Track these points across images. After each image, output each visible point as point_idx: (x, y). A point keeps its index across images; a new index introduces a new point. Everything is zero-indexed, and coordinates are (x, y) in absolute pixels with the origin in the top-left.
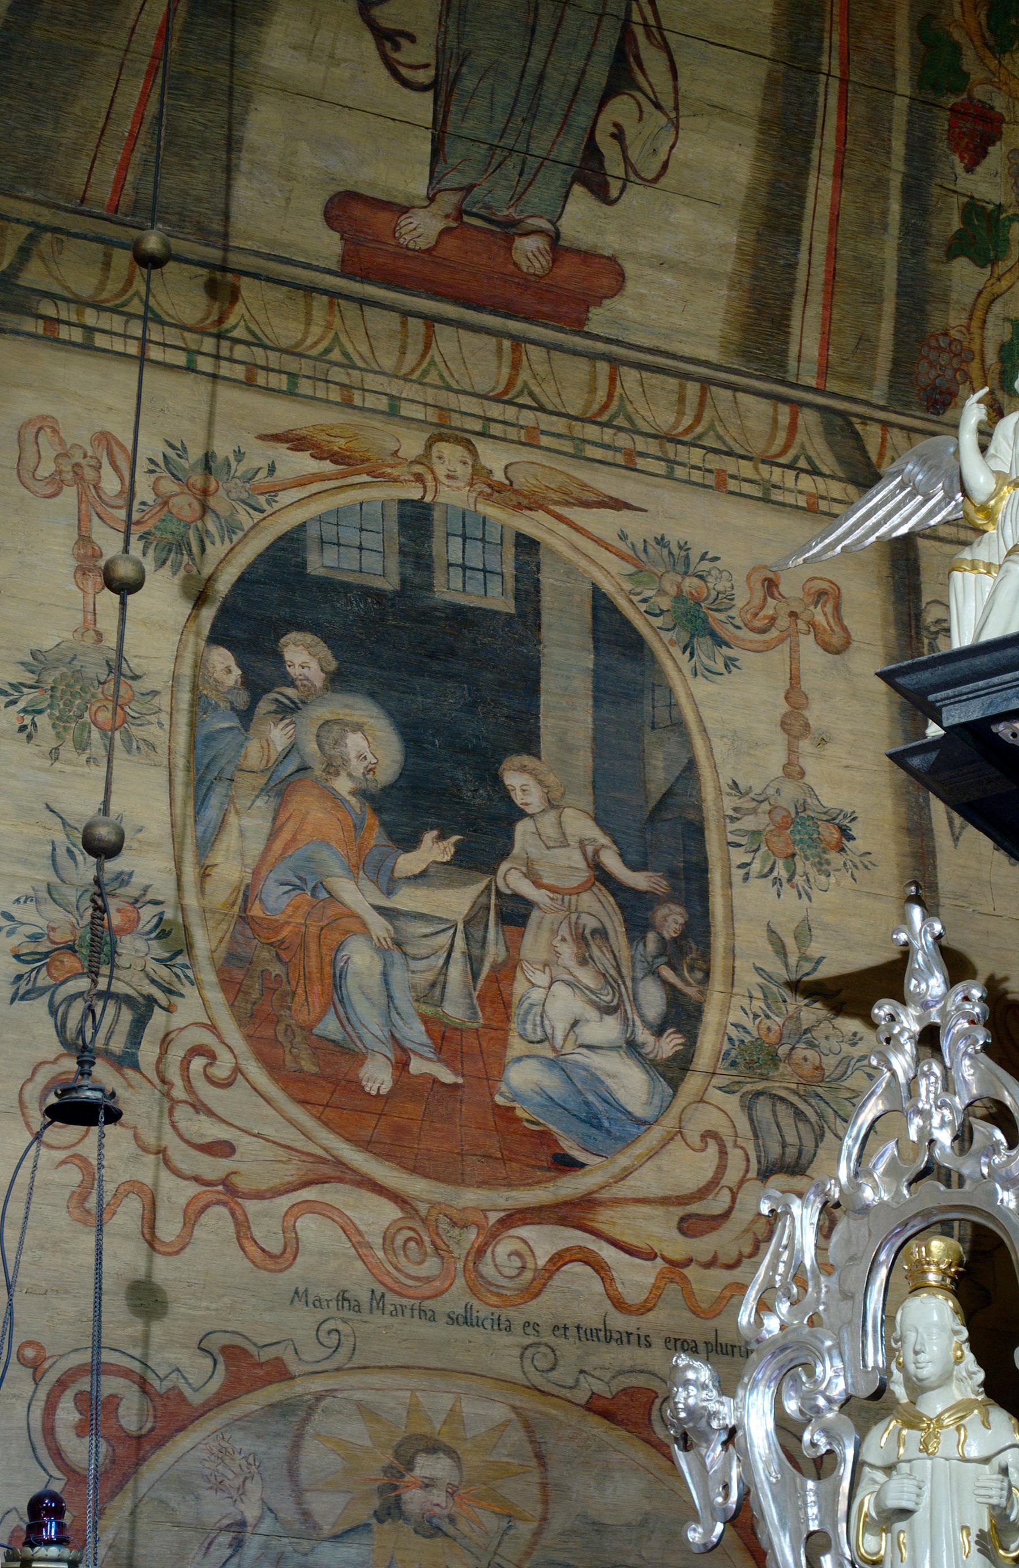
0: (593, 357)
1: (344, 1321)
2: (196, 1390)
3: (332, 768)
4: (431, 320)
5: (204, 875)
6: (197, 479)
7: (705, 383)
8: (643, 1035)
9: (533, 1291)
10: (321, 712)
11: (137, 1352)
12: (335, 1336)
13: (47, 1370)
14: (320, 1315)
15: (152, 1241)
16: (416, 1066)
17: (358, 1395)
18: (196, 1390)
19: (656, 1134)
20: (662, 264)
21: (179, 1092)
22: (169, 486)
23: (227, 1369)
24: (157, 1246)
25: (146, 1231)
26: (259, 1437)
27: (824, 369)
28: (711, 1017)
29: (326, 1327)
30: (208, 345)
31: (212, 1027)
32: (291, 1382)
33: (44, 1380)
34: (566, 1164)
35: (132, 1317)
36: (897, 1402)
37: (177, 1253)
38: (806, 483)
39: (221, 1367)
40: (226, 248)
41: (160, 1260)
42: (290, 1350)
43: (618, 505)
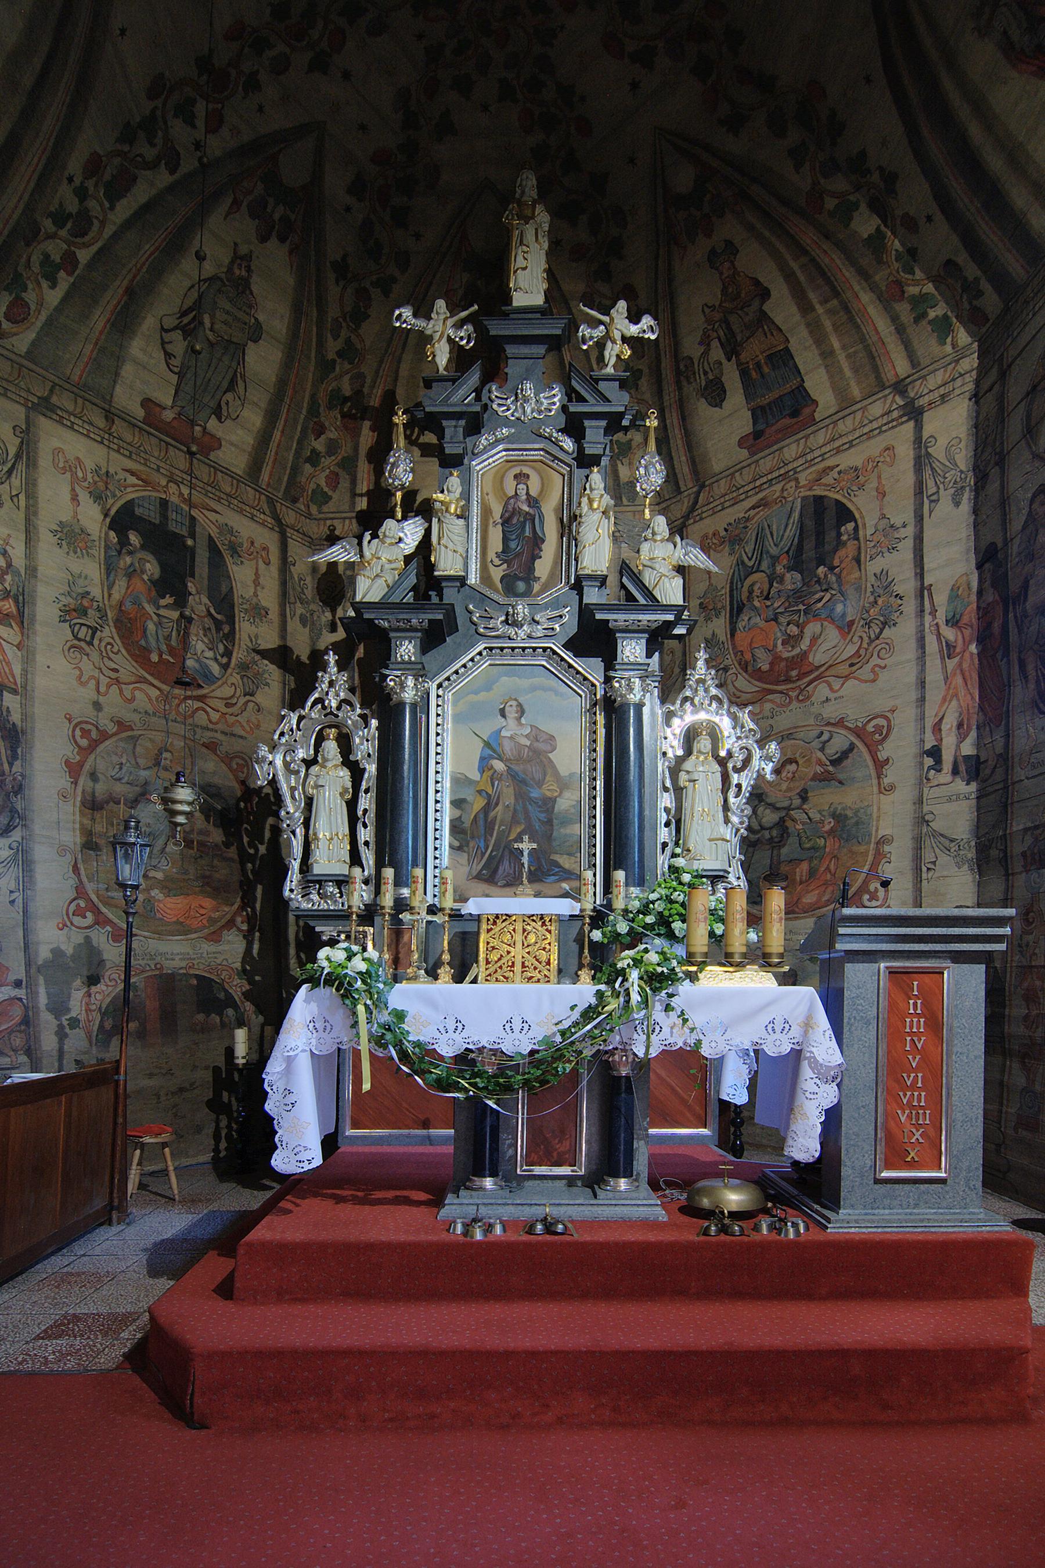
0: (210, 466)
3: (143, 572)
4: (167, 444)
5: (110, 595)
6: (104, 478)
7: (238, 480)
8: (219, 657)
10: (139, 555)
15: (98, 692)
16: (164, 656)
19: (220, 682)
20: (232, 444)
22: (97, 479)
27: (268, 485)
28: (235, 654)
30: (106, 436)
34: (200, 687)
38: (262, 516)
40: (110, 405)
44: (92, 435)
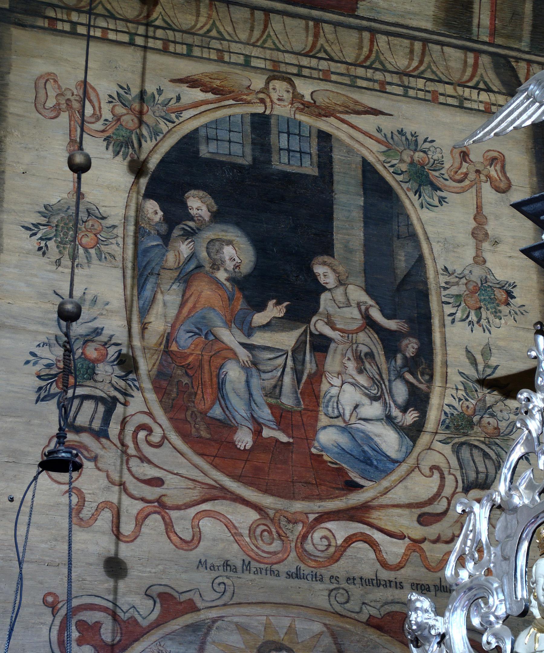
1: (228, 577)
2: (144, 618)
3: (216, 266)
5: (144, 328)
6: (136, 106)
7: (425, 42)
8: (396, 412)
9: (335, 558)
10: (209, 235)
11: (111, 598)
12: (222, 586)
13: (60, 609)
14: (214, 574)
15: (118, 535)
16: (266, 433)
17: (236, 619)
18: (144, 618)
19: (403, 468)
21: (132, 451)
22: (120, 110)
23: (161, 606)
24: (121, 538)
25: (114, 529)
26: (180, 644)
27: (493, 32)
28: (435, 401)
29: (217, 581)
30: (141, 30)
31: (150, 414)
32: (198, 613)
33: (59, 614)
34: (354, 486)
35: (109, 578)
36: (534, 618)
37: (132, 541)
38: (484, 96)
39: (158, 605)
41: (122, 546)
42: (197, 595)
43: (376, 112)
44: (112, 36)
